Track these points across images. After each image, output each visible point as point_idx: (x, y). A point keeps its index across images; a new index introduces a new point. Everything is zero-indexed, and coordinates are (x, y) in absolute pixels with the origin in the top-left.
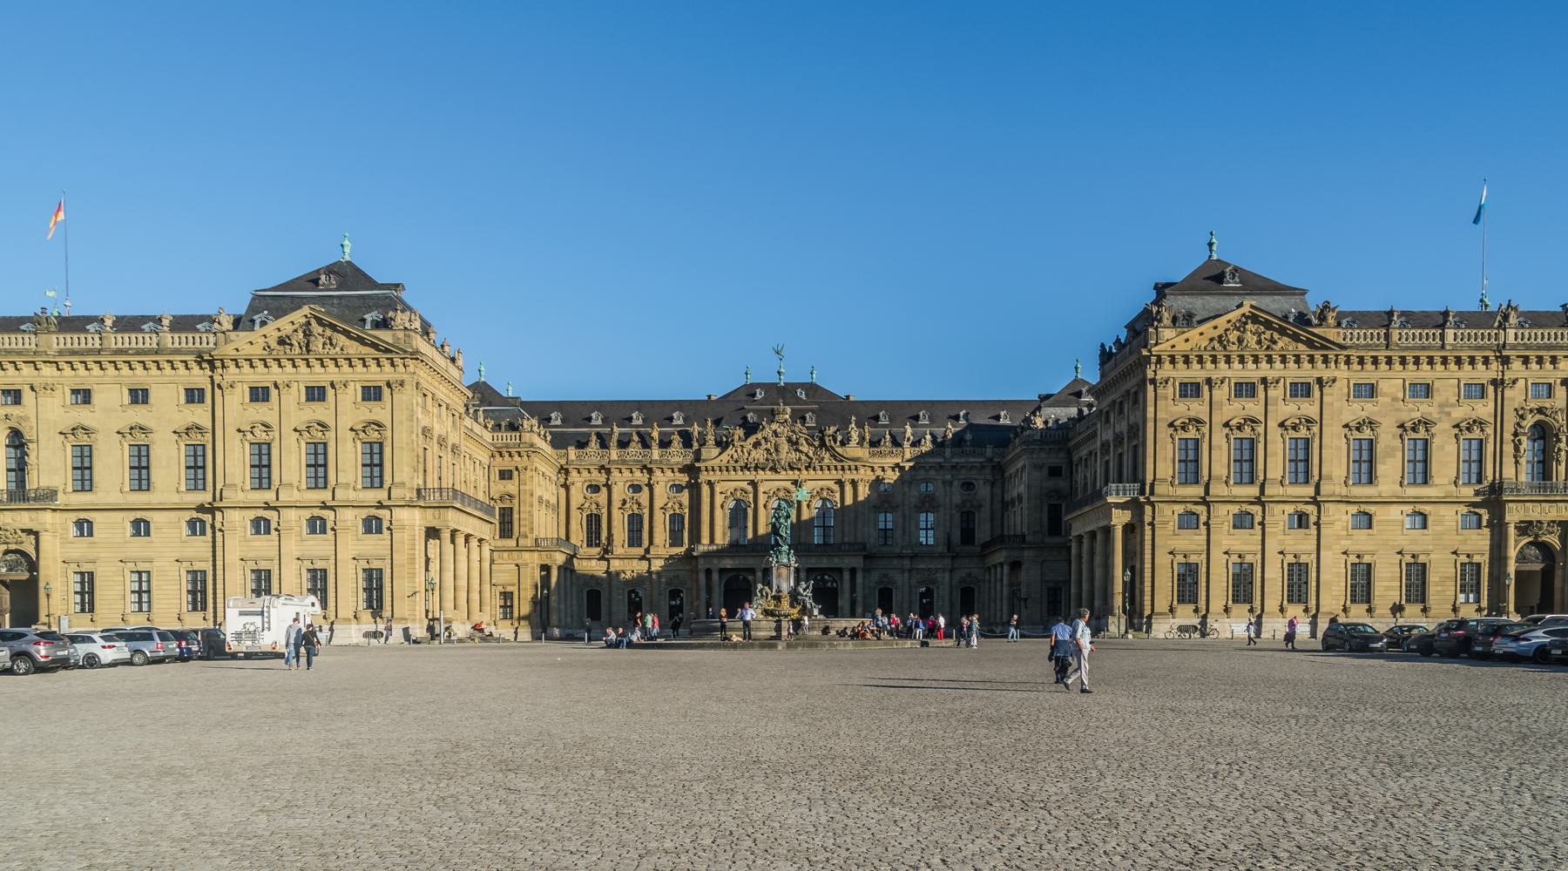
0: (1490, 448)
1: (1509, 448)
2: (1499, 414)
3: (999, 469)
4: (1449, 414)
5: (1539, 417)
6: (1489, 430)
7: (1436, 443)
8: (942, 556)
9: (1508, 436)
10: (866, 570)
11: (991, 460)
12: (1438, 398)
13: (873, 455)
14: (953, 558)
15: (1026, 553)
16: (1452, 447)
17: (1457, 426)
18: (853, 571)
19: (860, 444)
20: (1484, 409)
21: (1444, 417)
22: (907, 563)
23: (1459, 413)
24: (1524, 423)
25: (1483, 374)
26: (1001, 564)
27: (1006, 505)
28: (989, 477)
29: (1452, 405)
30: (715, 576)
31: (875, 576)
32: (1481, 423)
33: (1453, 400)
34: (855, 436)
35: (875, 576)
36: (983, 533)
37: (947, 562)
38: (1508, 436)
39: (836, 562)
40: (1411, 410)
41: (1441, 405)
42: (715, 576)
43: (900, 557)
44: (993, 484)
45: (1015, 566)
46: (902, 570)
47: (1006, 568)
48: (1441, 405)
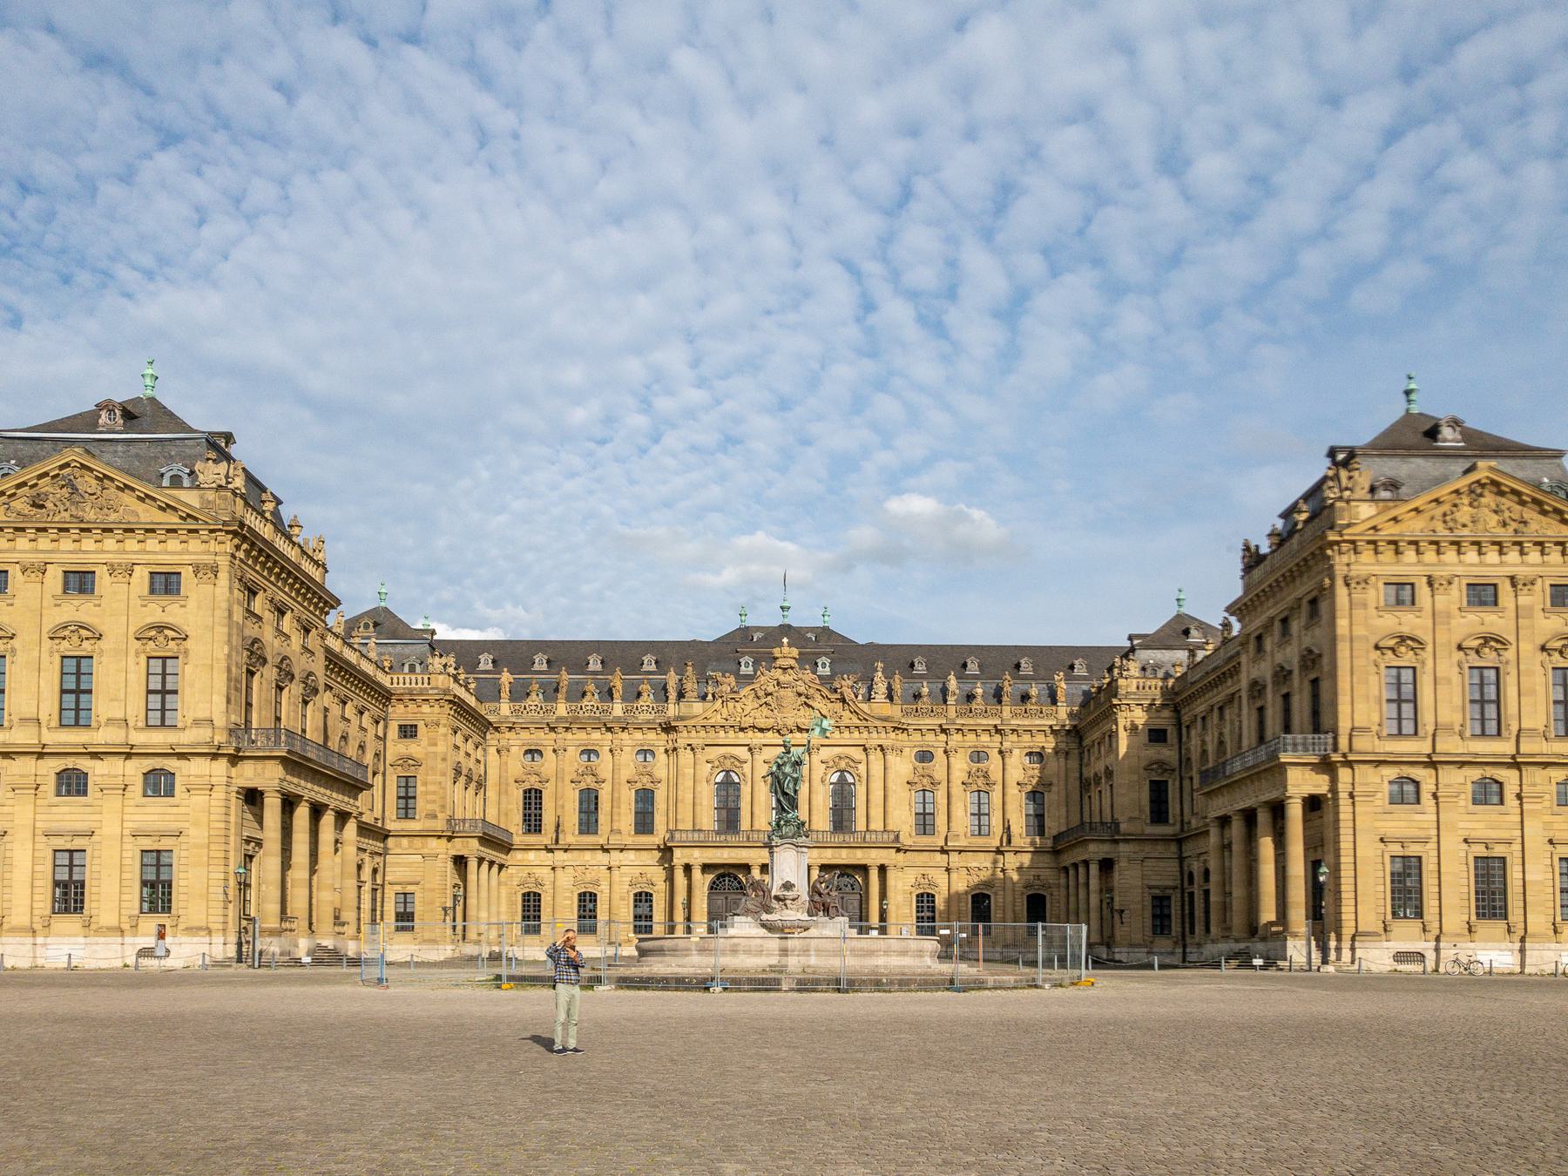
15: (1123, 847)
18: (883, 869)
19: (890, 697)
26: (1086, 863)
34: (881, 688)
39: (858, 857)
45: (1107, 865)
47: (1094, 869)
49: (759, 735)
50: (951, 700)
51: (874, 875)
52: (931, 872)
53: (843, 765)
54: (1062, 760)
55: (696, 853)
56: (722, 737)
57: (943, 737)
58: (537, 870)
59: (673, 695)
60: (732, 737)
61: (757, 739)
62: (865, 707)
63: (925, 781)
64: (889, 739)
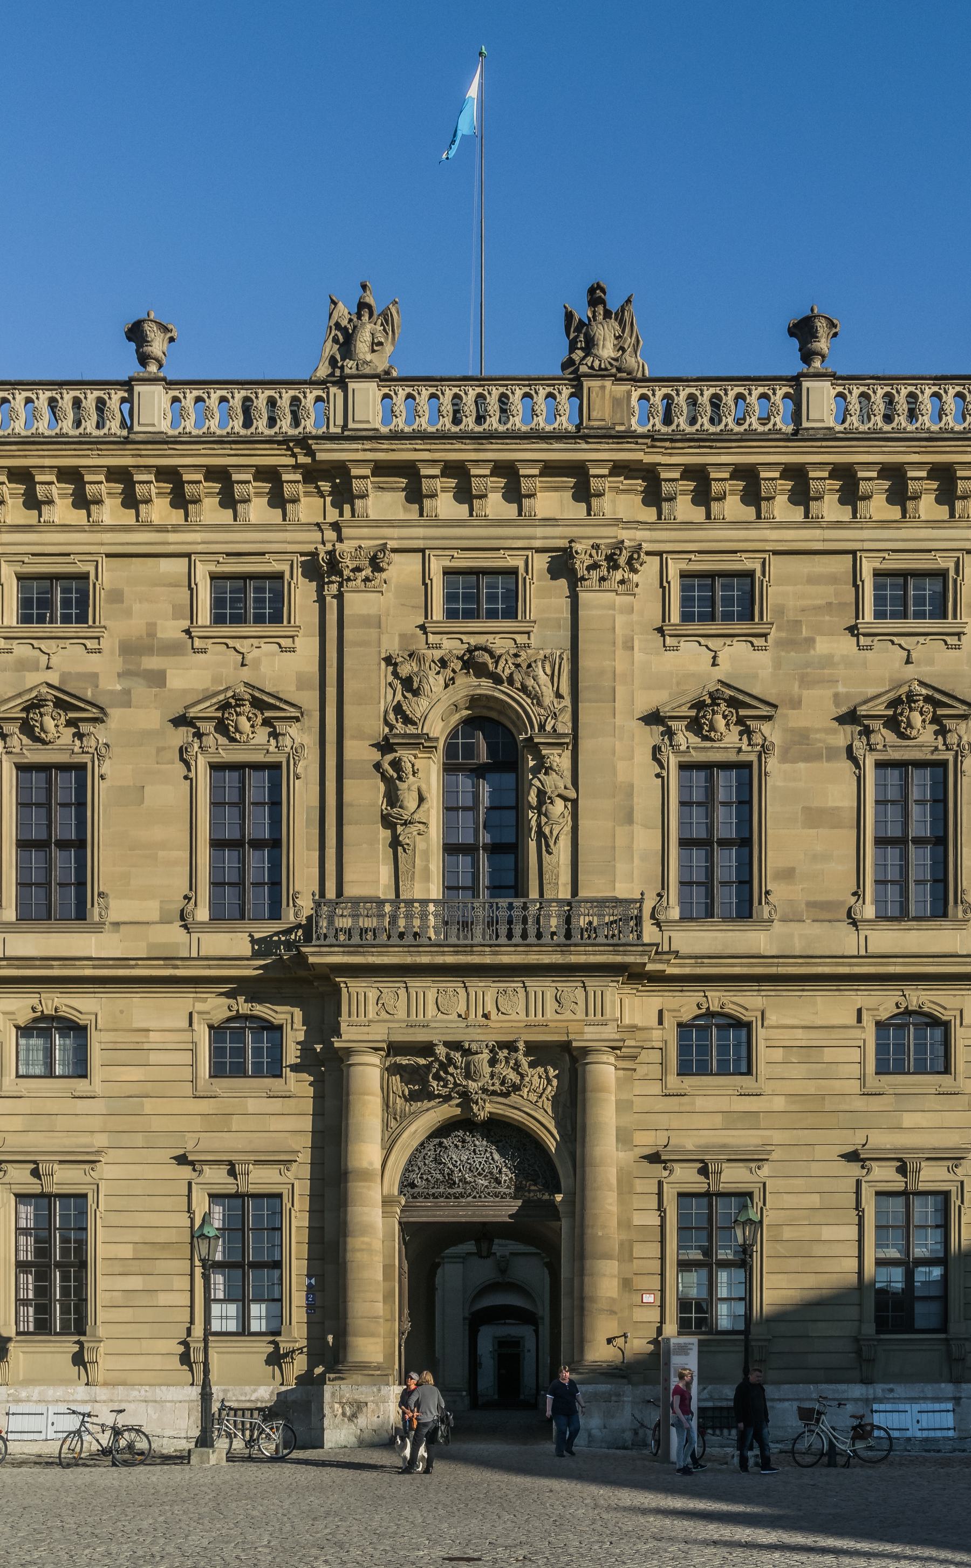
0: (302, 796)
1: (365, 794)
2: (331, 676)
4: (158, 679)
5: (468, 684)
6: (301, 735)
7: (111, 778)
9: (360, 752)
12: (114, 625)
16: (168, 793)
17: (181, 721)
20: (283, 662)
21: (141, 691)
23: (198, 675)
24: (417, 707)
25: (271, 533)
29: (171, 649)
32: (264, 704)
33: (172, 629)
38: (360, 752)
40: (23, 666)
41: (129, 649)
48: (129, 649)
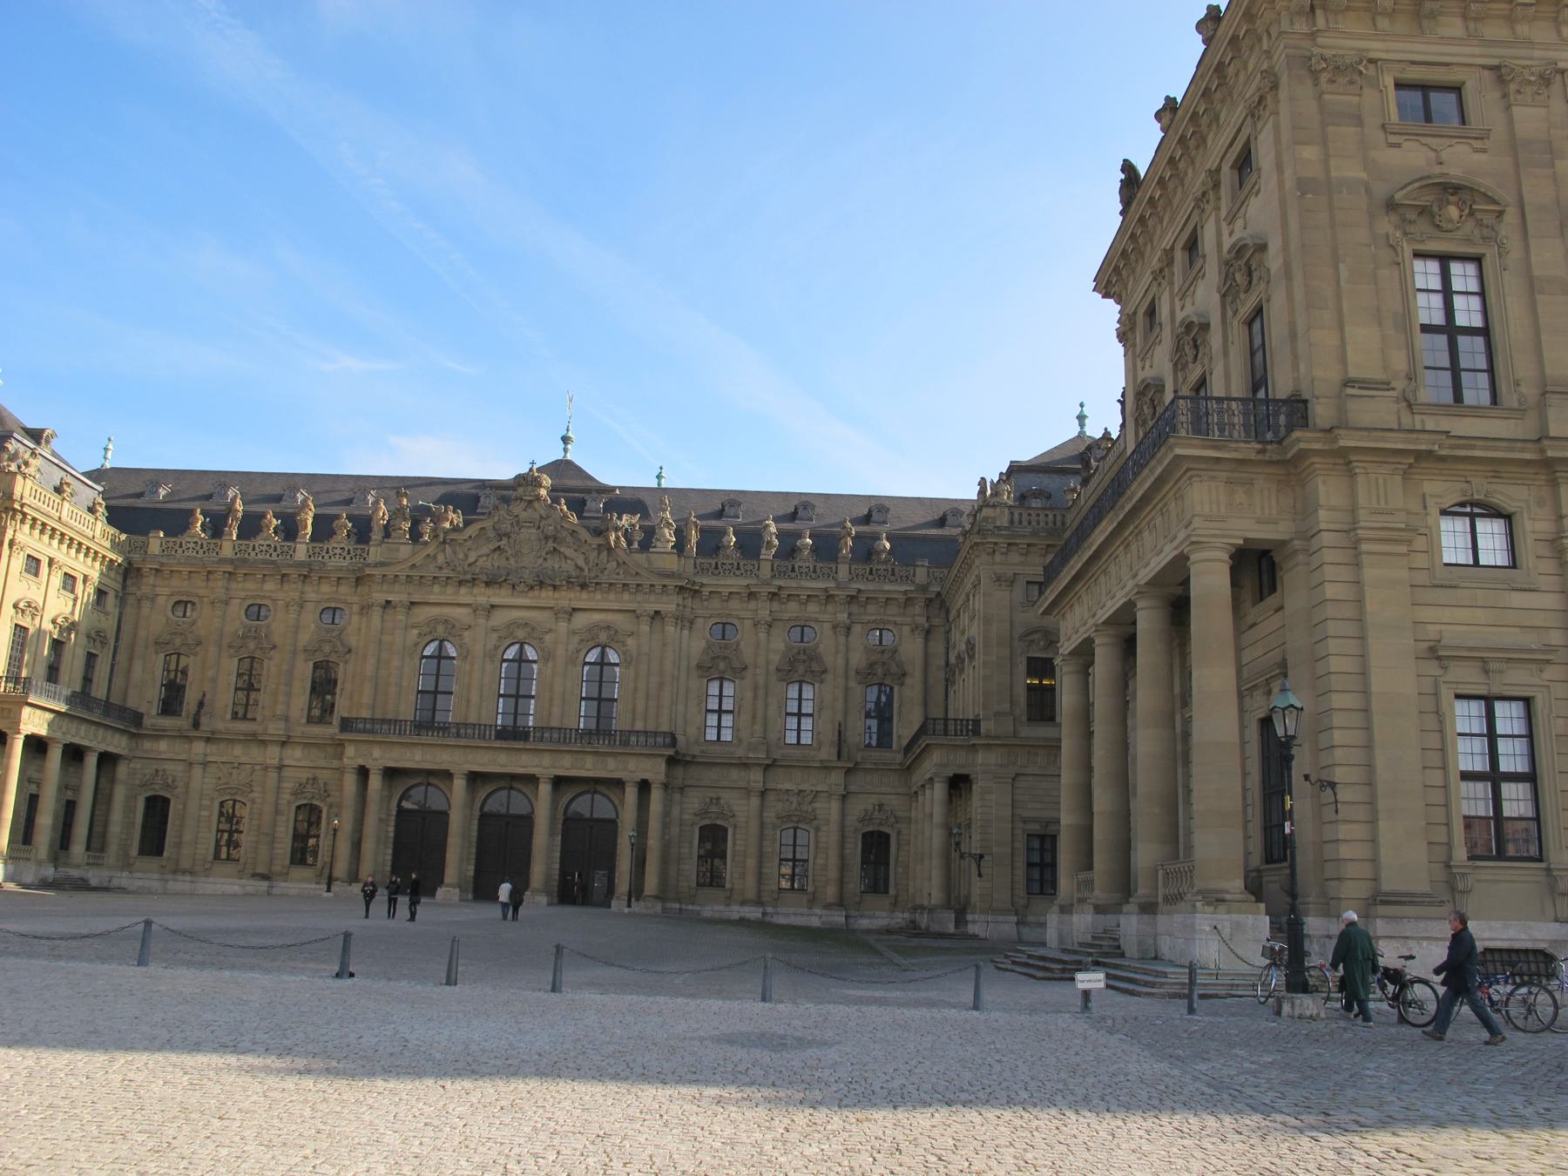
3: (938, 604)
8: (825, 768)
10: (666, 786)
11: (924, 588)
13: (703, 570)
14: (848, 771)
18: (644, 786)
19: (680, 546)
22: (756, 777)
27: (951, 672)
28: (922, 620)
30: (375, 782)
31: (693, 802)
35: (693, 802)
36: (904, 727)
37: (836, 778)
39: (610, 768)
42: (375, 782)
43: (744, 765)
44: (928, 633)
46: (748, 792)
49: (490, 591)
50: (767, 554)
51: (631, 794)
52: (726, 796)
53: (603, 637)
54: (919, 641)
55: (377, 752)
56: (436, 593)
57: (752, 605)
58: (169, 767)
59: (376, 535)
60: (449, 594)
61: (483, 596)
62: (641, 558)
63: (722, 665)
64: (669, 605)
